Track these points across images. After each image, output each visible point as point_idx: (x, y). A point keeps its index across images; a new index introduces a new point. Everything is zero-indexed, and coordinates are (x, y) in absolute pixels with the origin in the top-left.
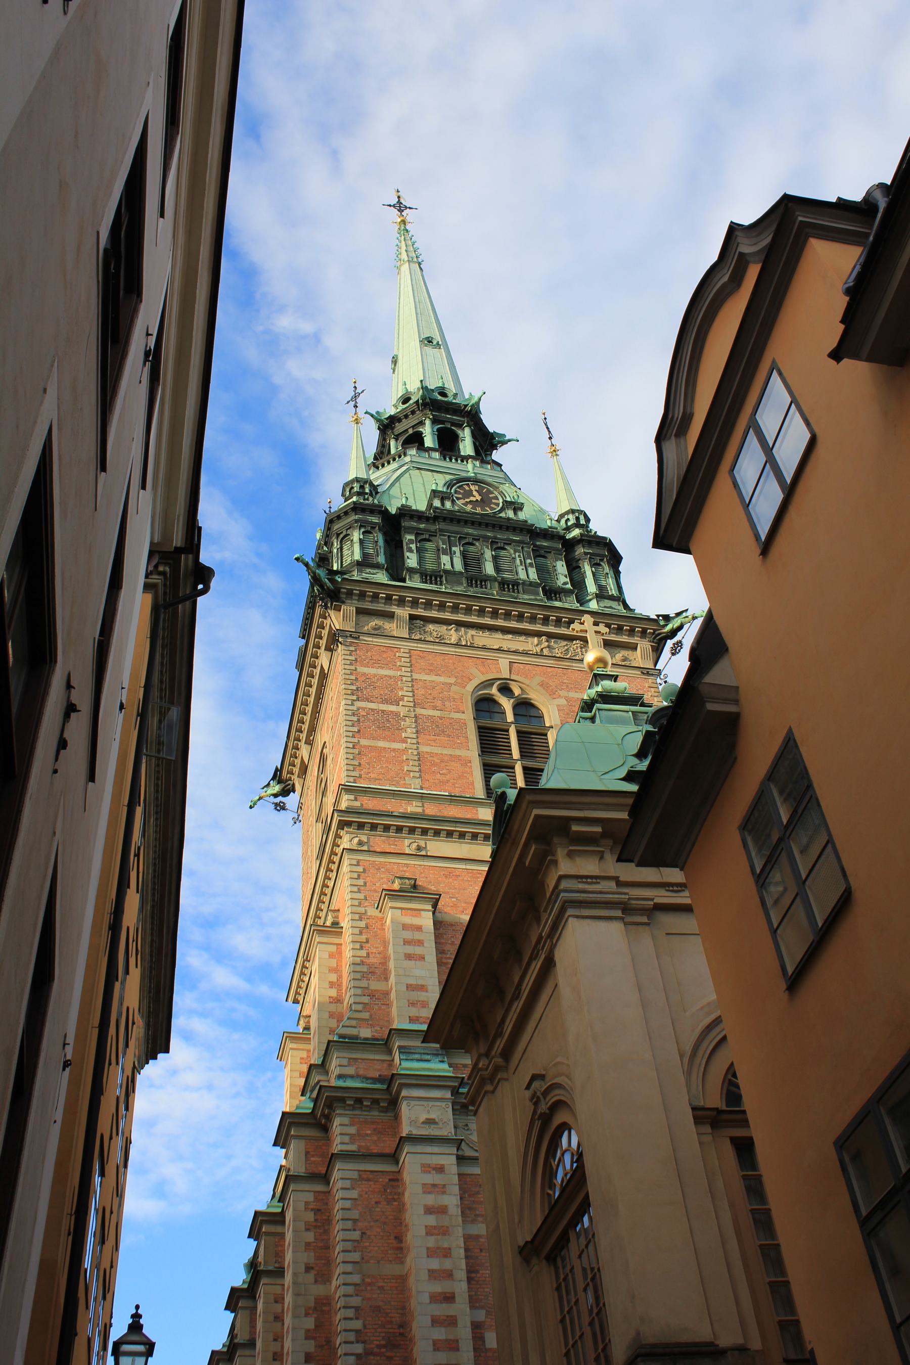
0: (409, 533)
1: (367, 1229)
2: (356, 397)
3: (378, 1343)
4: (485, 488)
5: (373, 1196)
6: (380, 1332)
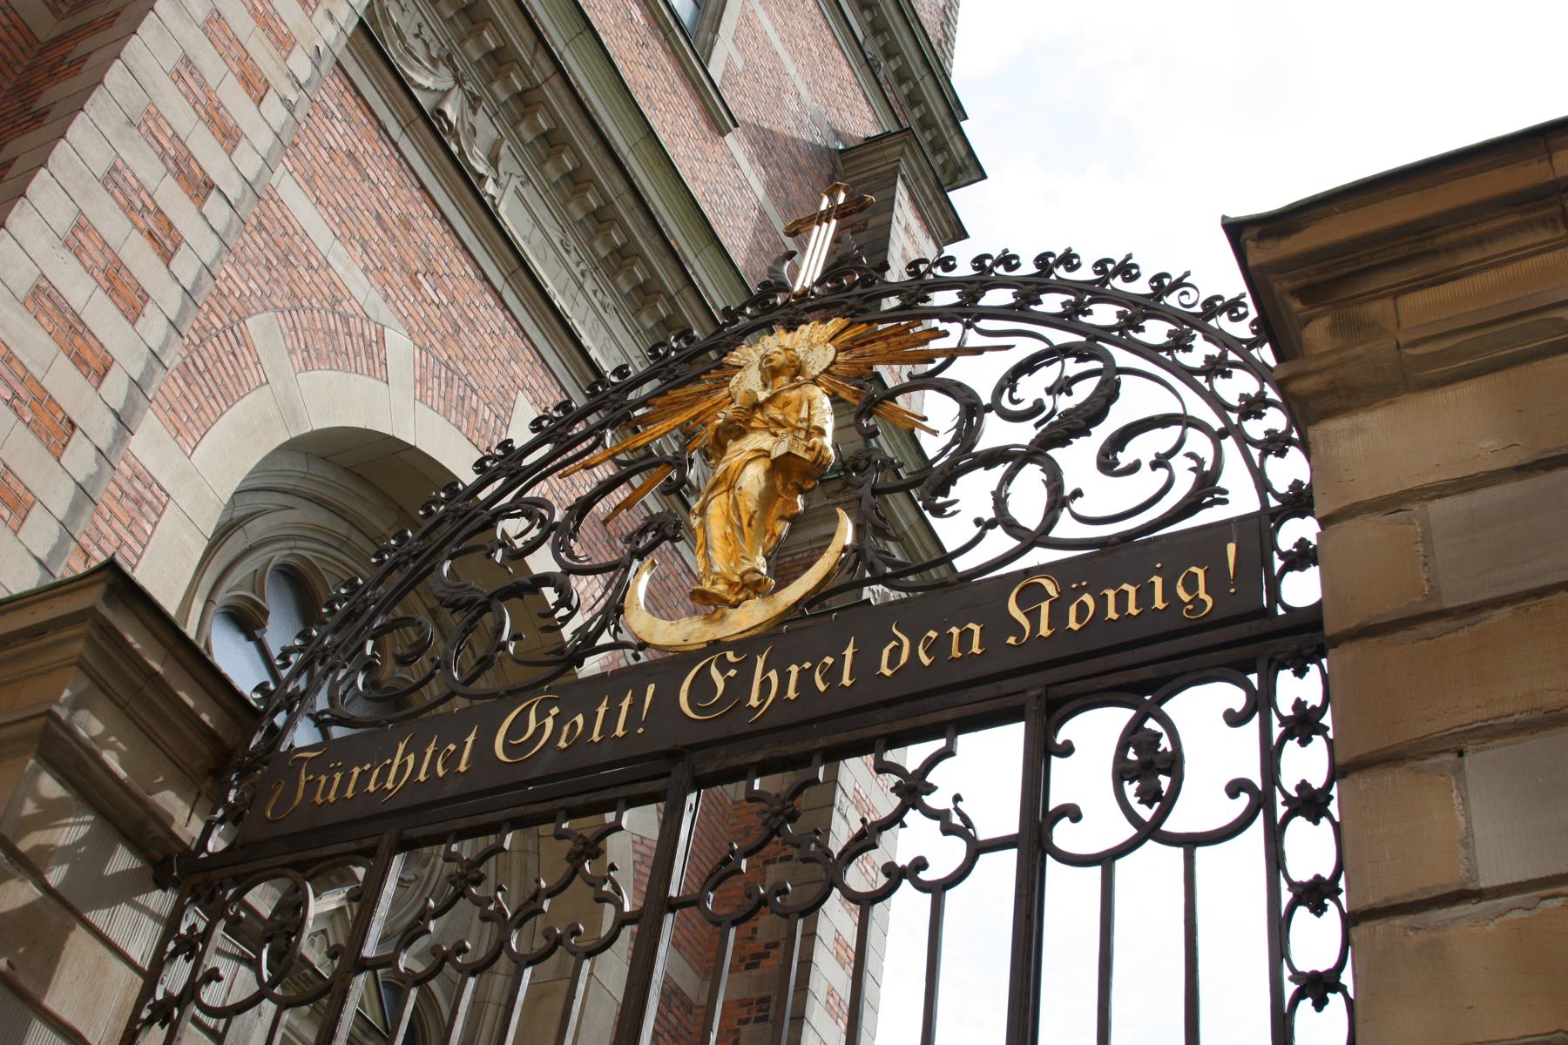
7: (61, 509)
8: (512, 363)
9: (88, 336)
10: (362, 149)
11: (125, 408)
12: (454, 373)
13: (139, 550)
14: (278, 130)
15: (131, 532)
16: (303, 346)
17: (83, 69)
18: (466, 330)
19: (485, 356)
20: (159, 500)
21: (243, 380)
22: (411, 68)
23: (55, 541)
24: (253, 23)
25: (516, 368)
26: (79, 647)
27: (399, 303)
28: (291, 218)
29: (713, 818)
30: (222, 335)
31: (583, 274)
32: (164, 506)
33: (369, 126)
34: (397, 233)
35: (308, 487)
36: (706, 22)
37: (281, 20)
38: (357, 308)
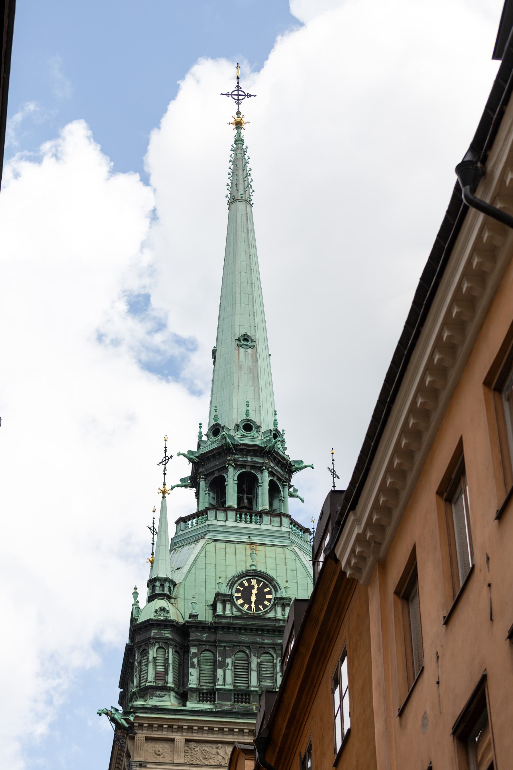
0: (194, 646)
2: (165, 460)
4: (262, 581)
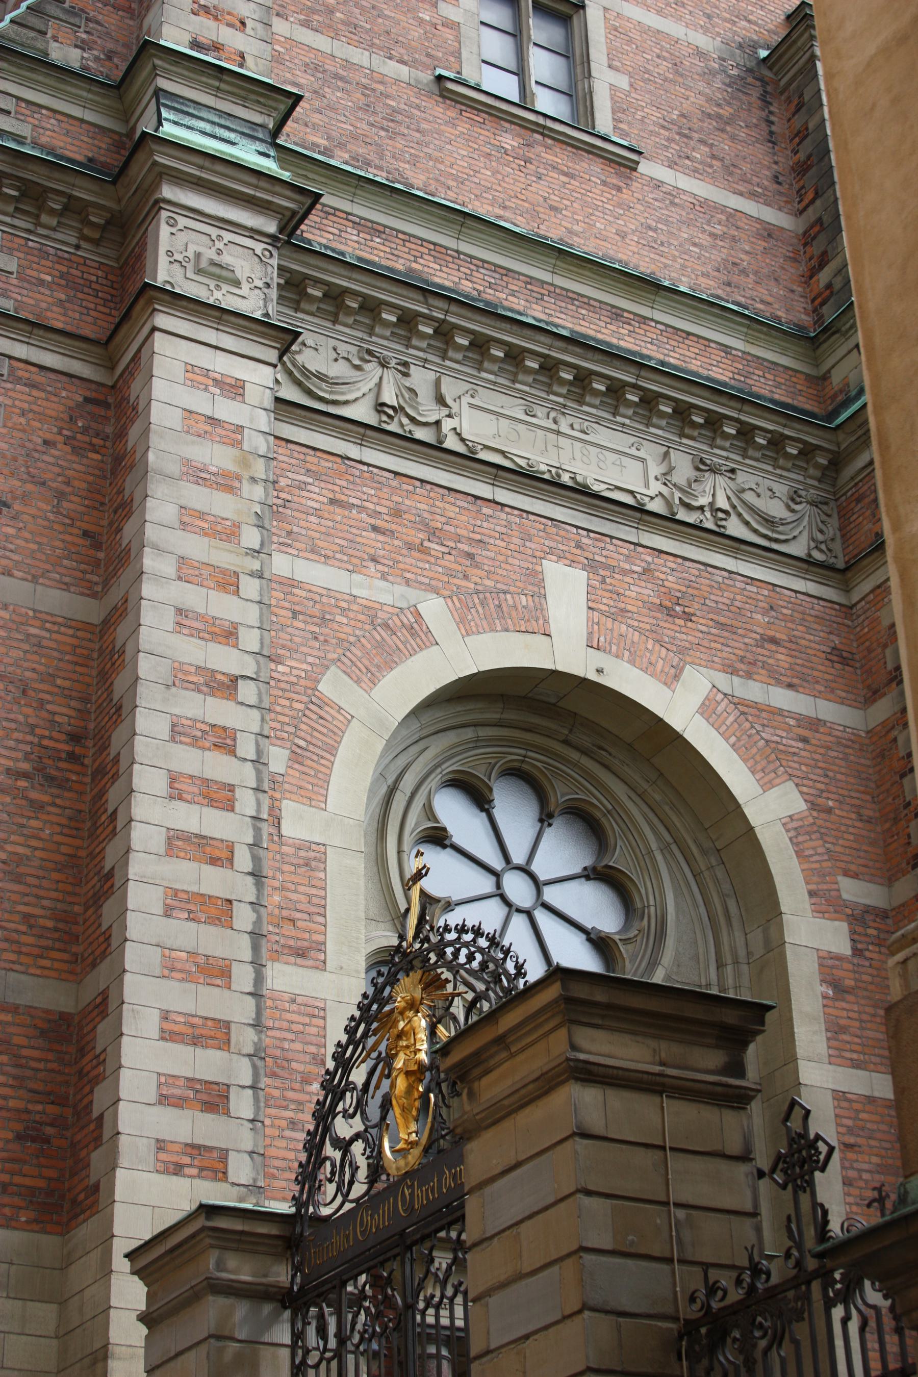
1: (14, 498)
3: (10, 764)
5: (38, 425)
6: (17, 741)
7: (247, 955)
8: (528, 544)
9: (211, 842)
10: (337, 489)
11: (254, 866)
12: (483, 592)
13: (322, 893)
14: (258, 599)
15: (313, 886)
16: (364, 670)
17: (127, 661)
18: (479, 551)
19: (501, 558)
20: (319, 852)
21: (335, 730)
22: (342, 393)
23: (253, 975)
24: (206, 539)
25: (533, 546)
26: (208, 1241)
27: (420, 578)
28: (314, 589)
29: (852, 758)
30: (307, 712)
31: (555, 422)
32: (325, 854)
33: (335, 466)
34: (393, 527)
35: (425, 732)
36: (579, 70)
37: (223, 519)
38: (390, 609)
